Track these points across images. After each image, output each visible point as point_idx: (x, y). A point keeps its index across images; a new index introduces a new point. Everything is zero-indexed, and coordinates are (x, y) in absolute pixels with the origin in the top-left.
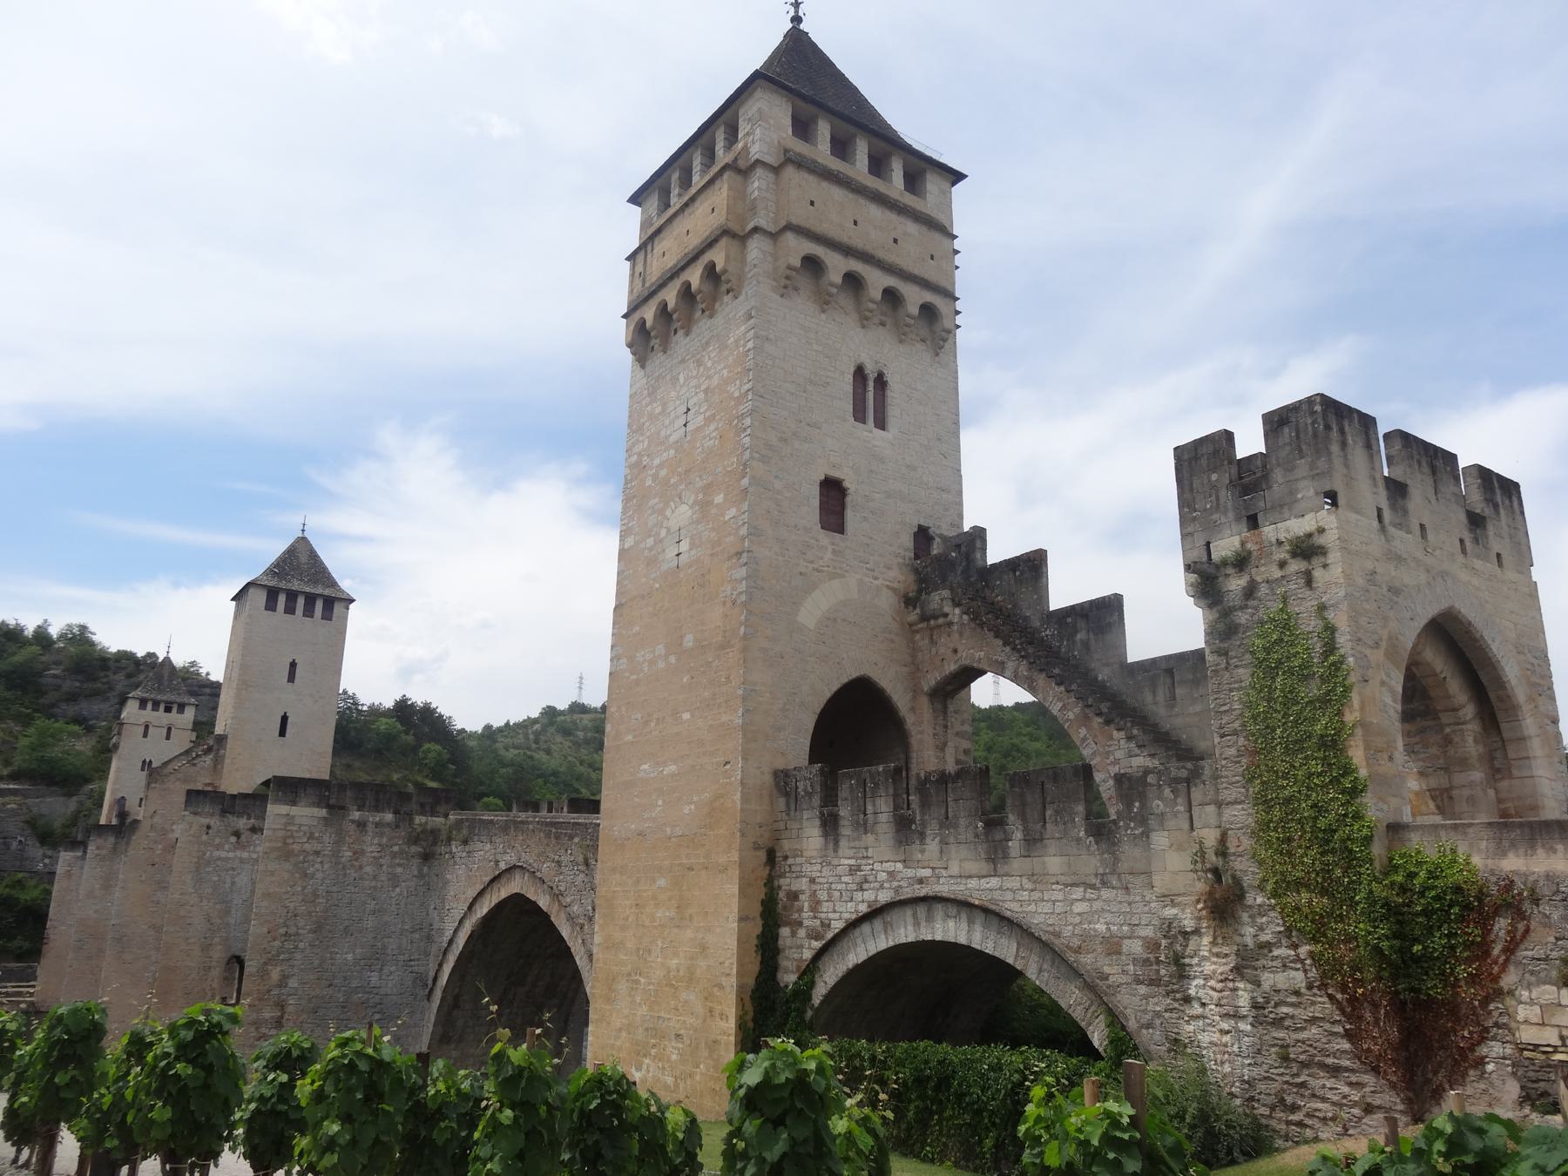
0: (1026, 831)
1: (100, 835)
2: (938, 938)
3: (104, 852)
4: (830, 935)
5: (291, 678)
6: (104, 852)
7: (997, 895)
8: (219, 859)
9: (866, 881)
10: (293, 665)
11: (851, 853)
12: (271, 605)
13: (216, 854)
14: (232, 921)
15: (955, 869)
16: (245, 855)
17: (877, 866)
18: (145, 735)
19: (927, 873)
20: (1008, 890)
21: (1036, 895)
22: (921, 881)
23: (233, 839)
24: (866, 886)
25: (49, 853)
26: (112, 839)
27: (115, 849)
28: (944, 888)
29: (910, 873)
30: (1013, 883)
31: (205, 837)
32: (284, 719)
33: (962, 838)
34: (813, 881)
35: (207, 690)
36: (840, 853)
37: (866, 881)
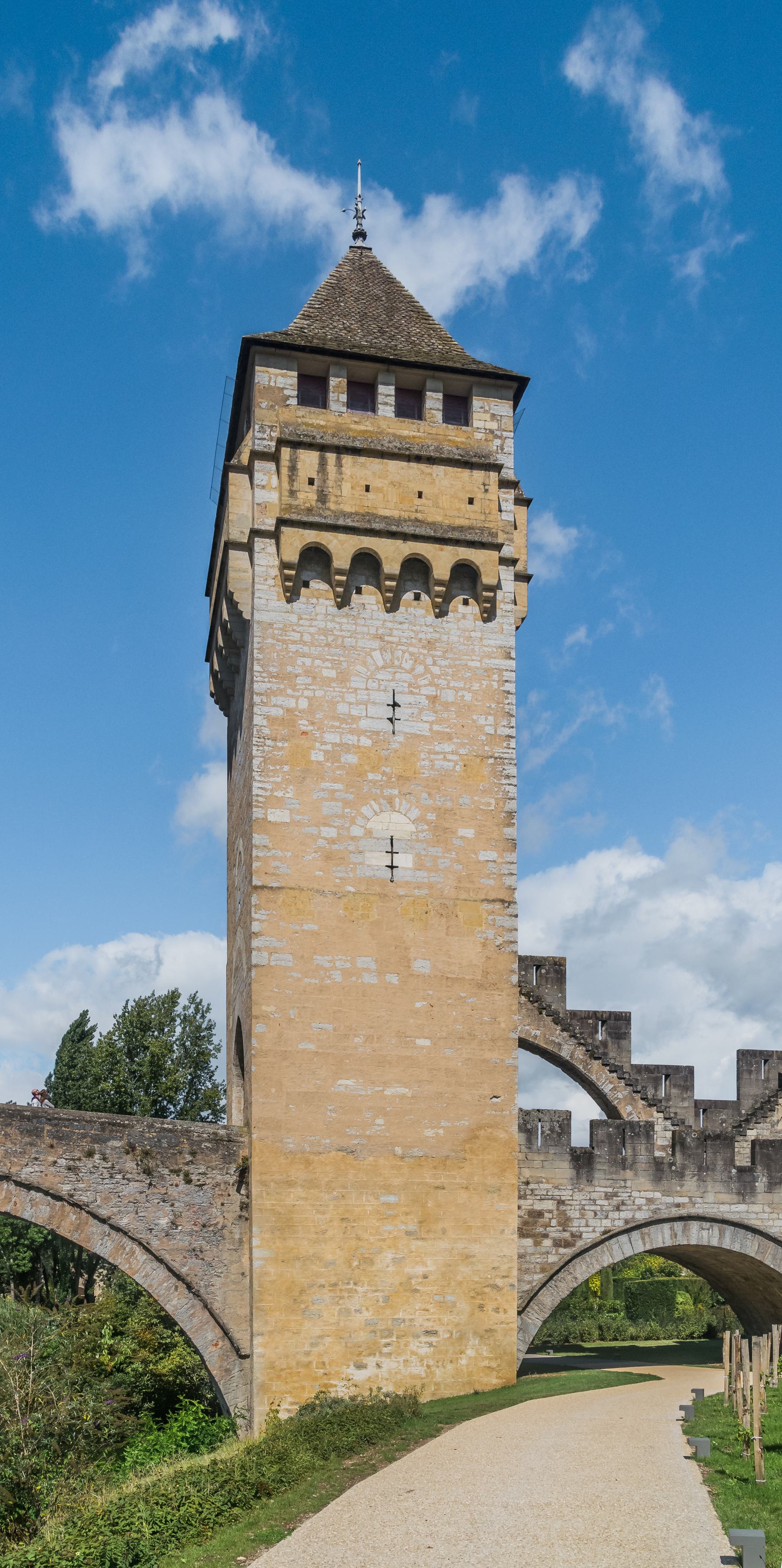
0: (770, 1177)
2: (693, 1242)
4: (580, 1244)
7: (743, 1216)
9: (623, 1204)
11: (609, 1183)
15: (710, 1197)
17: (635, 1194)
19: (686, 1200)
20: (754, 1212)
21: (775, 1216)
22: (678, 1205)
24: (623, 1208)
28: (698, 1209)
29: (669, 1200)
30: (757, 1208)
33: (718, 1177)
34: (561, 1202)
36: (596, 1182)
37: (623, 1204)
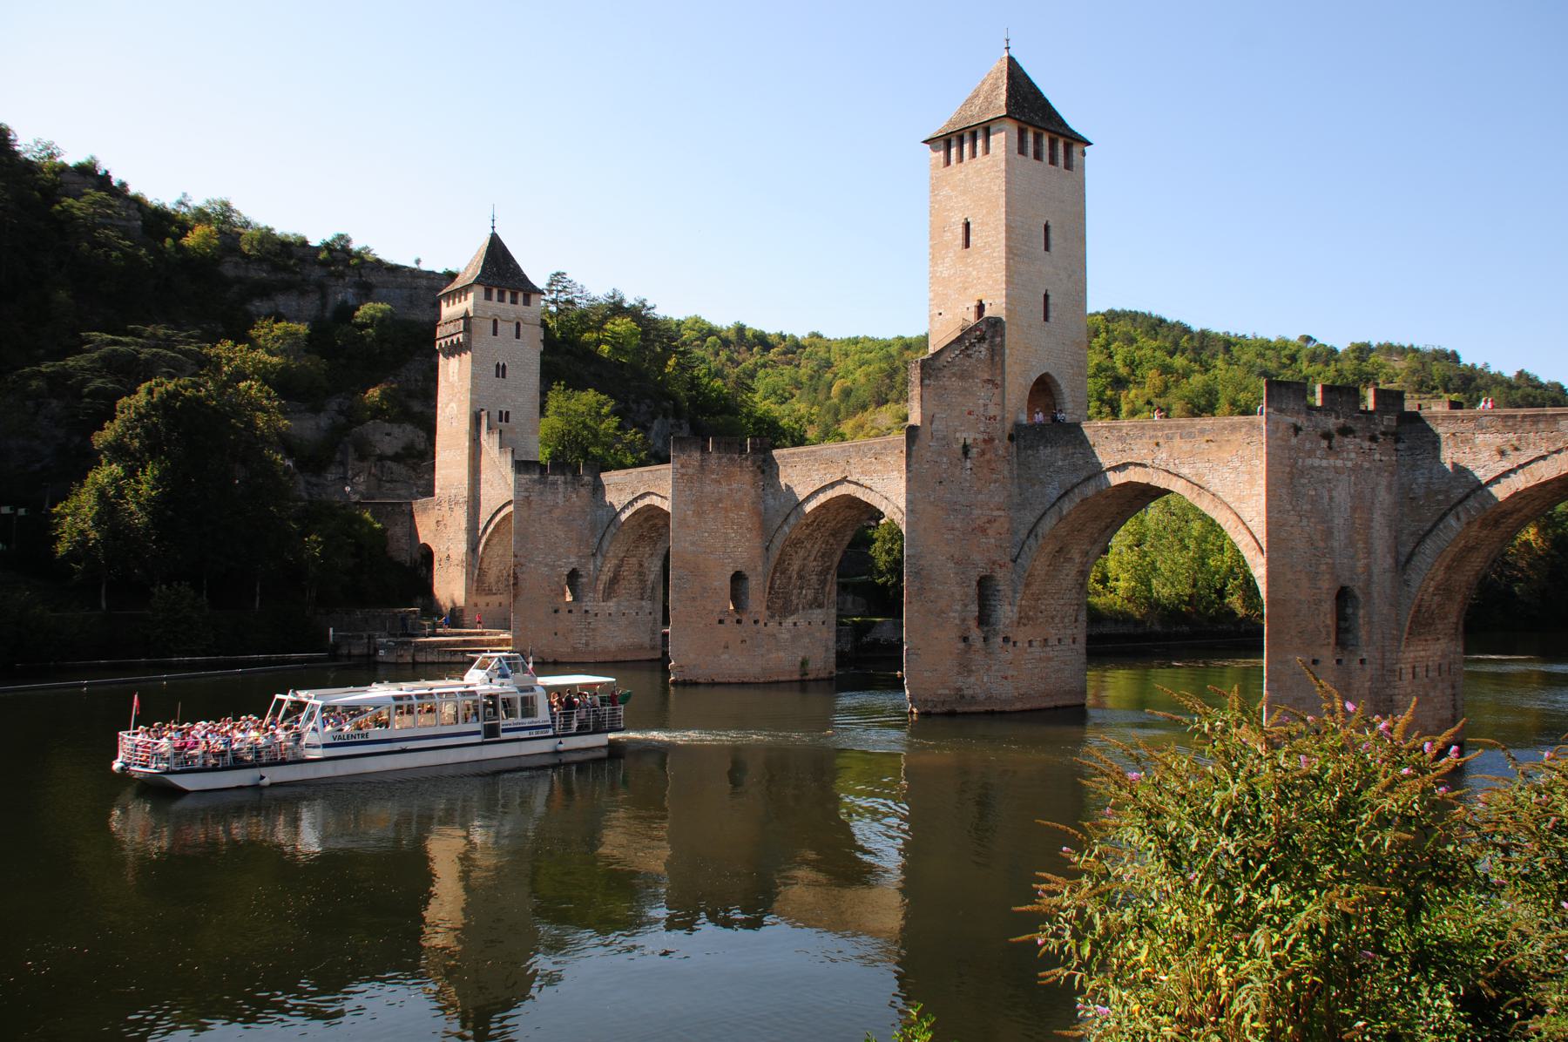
1: (682, 450)
3: (690, 471)
5: (1047, 248)
6: (690, 471)
8: (1313, 467)
10: (1047, 228)
12: (1022, 150)
13: (1309, 462)
14: (1336, 544)
16: (1339, 463)
18: (495, 333)
23: (1324, 444)
25: (313, 480)
26: (697, 455)
27: (702, 468)
31: (1294, 441)
32: (1046, 297)
35: (424, 282)
